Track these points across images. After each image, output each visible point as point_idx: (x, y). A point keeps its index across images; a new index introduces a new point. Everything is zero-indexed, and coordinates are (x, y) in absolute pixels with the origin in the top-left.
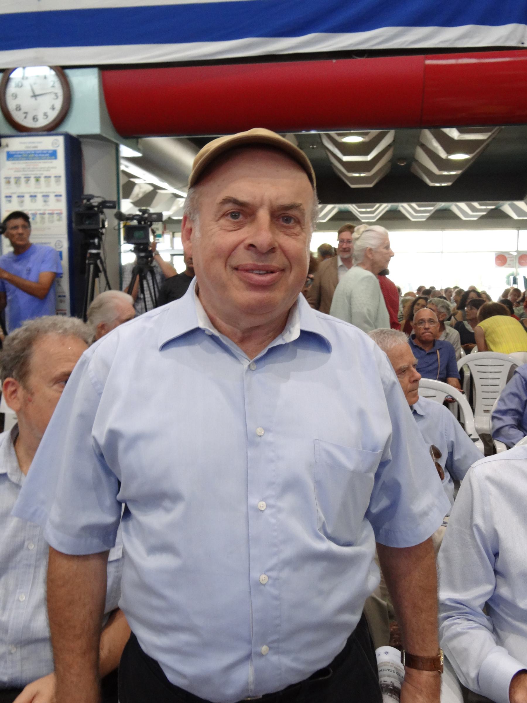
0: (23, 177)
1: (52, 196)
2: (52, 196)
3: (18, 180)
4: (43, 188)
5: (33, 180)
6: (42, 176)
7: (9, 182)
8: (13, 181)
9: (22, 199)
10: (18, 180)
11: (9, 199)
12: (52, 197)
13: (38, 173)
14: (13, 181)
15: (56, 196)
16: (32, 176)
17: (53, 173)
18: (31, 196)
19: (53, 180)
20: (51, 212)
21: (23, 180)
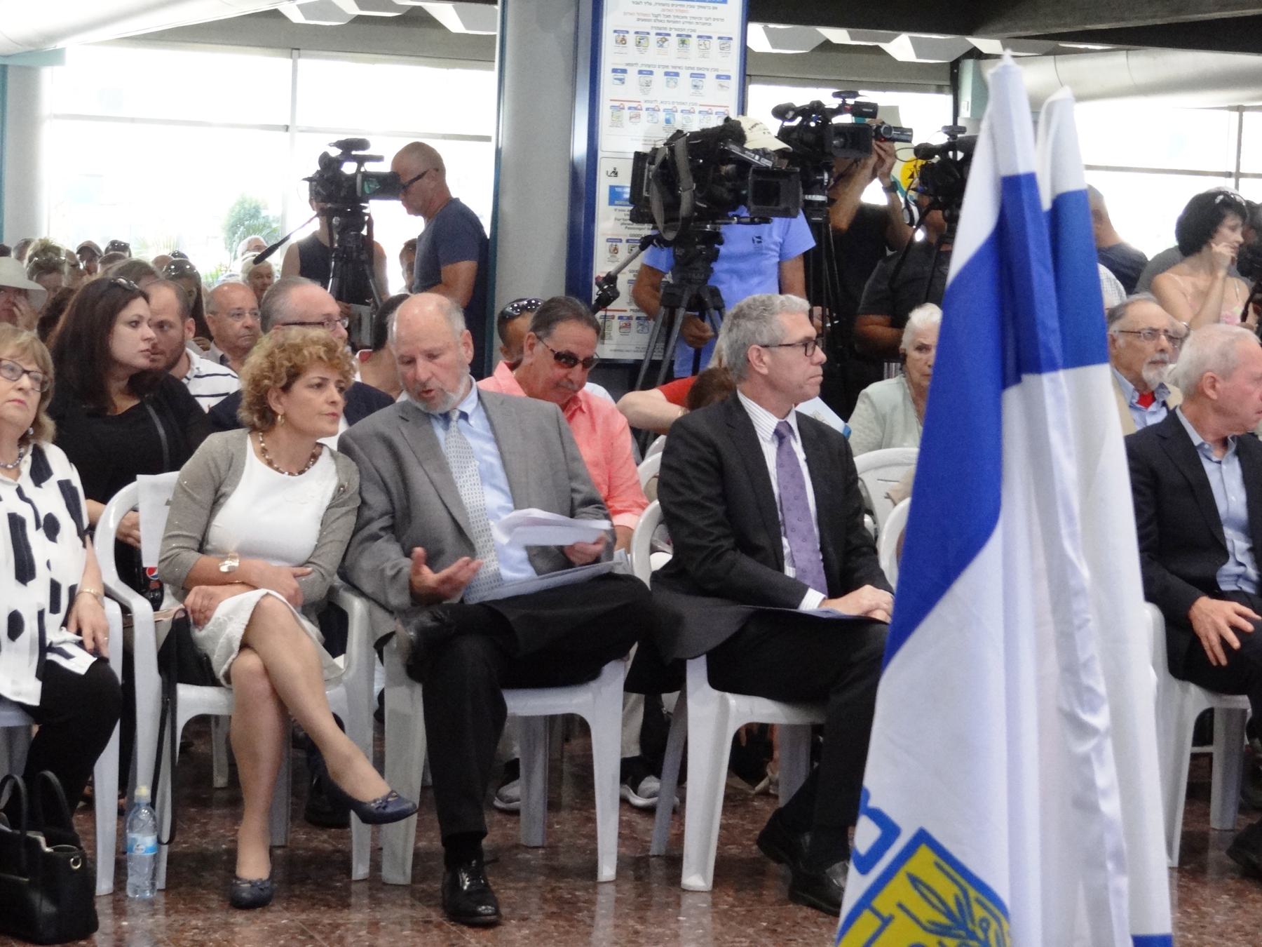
0: (653, 32)
1: (710, 76)
2: (710, 76)
3: (642, 37)
4: (693, 57)
5: (673, 41)
6: (694, 35)
7: (623, 41)
8: (631, 38)
9: (648, 78)
10: (642, 37)
11: (620, 76)
12: (710, 81)
13: (686, 28)
14: (631, 38)
15: (718, 77)
16: (674, 33)
17: (716, 30)
18: (667, 74)
19: (715, 43)
20: (706, 109)
21: (653, 39)
